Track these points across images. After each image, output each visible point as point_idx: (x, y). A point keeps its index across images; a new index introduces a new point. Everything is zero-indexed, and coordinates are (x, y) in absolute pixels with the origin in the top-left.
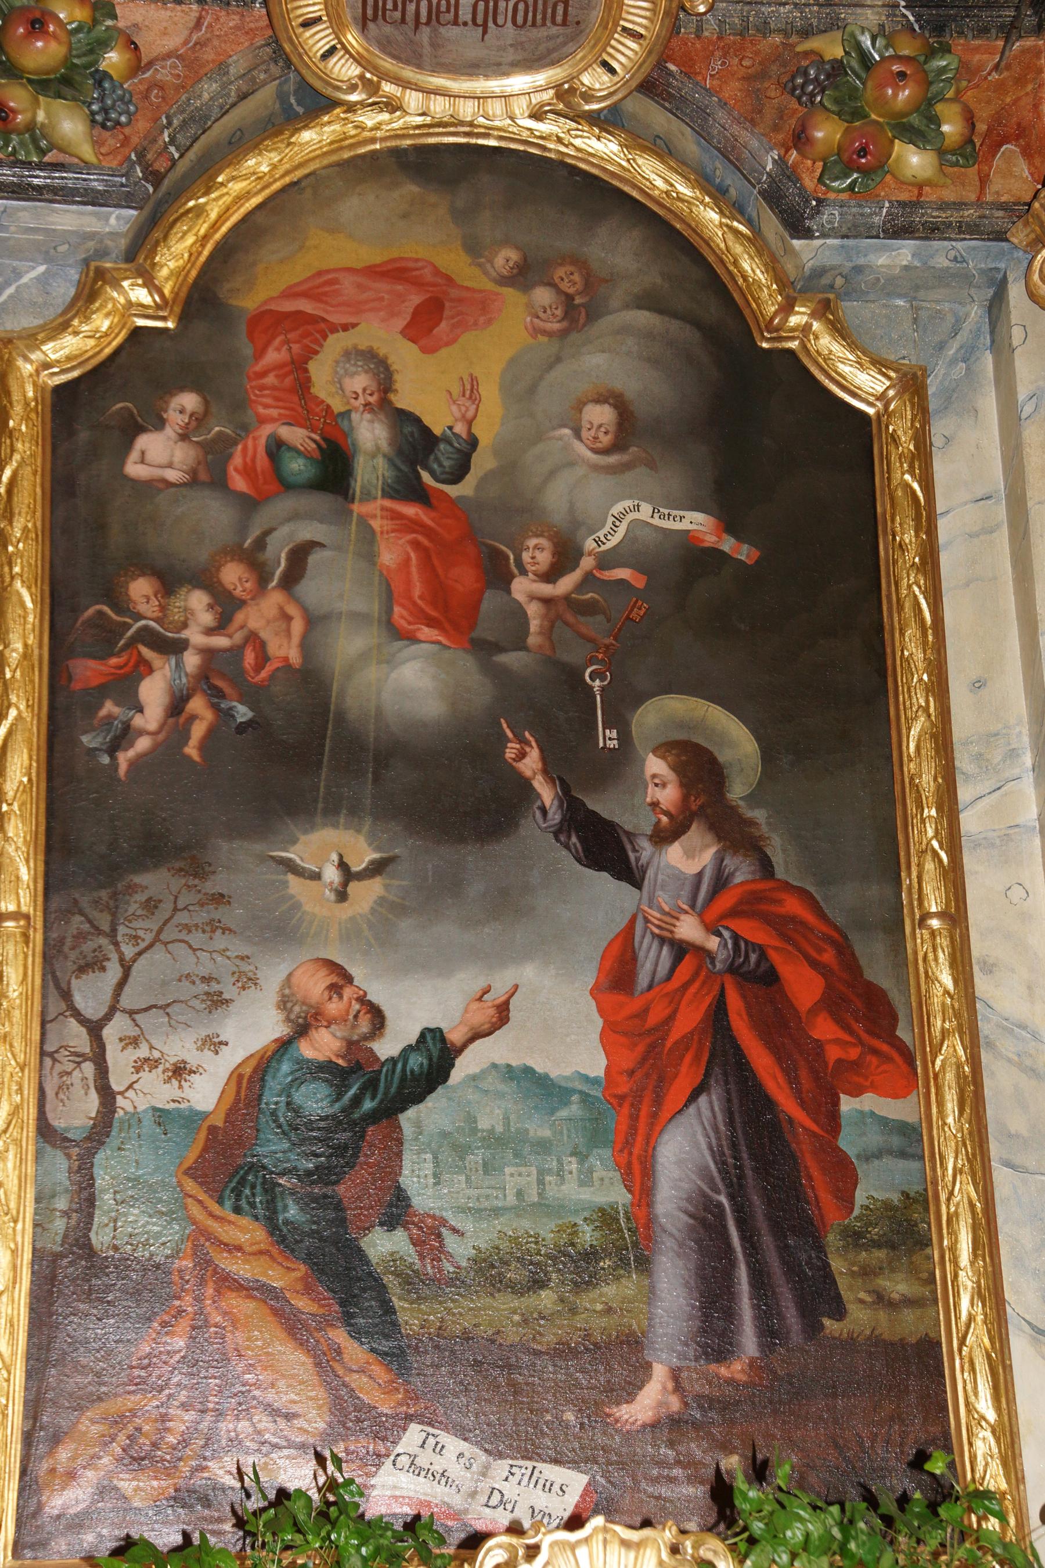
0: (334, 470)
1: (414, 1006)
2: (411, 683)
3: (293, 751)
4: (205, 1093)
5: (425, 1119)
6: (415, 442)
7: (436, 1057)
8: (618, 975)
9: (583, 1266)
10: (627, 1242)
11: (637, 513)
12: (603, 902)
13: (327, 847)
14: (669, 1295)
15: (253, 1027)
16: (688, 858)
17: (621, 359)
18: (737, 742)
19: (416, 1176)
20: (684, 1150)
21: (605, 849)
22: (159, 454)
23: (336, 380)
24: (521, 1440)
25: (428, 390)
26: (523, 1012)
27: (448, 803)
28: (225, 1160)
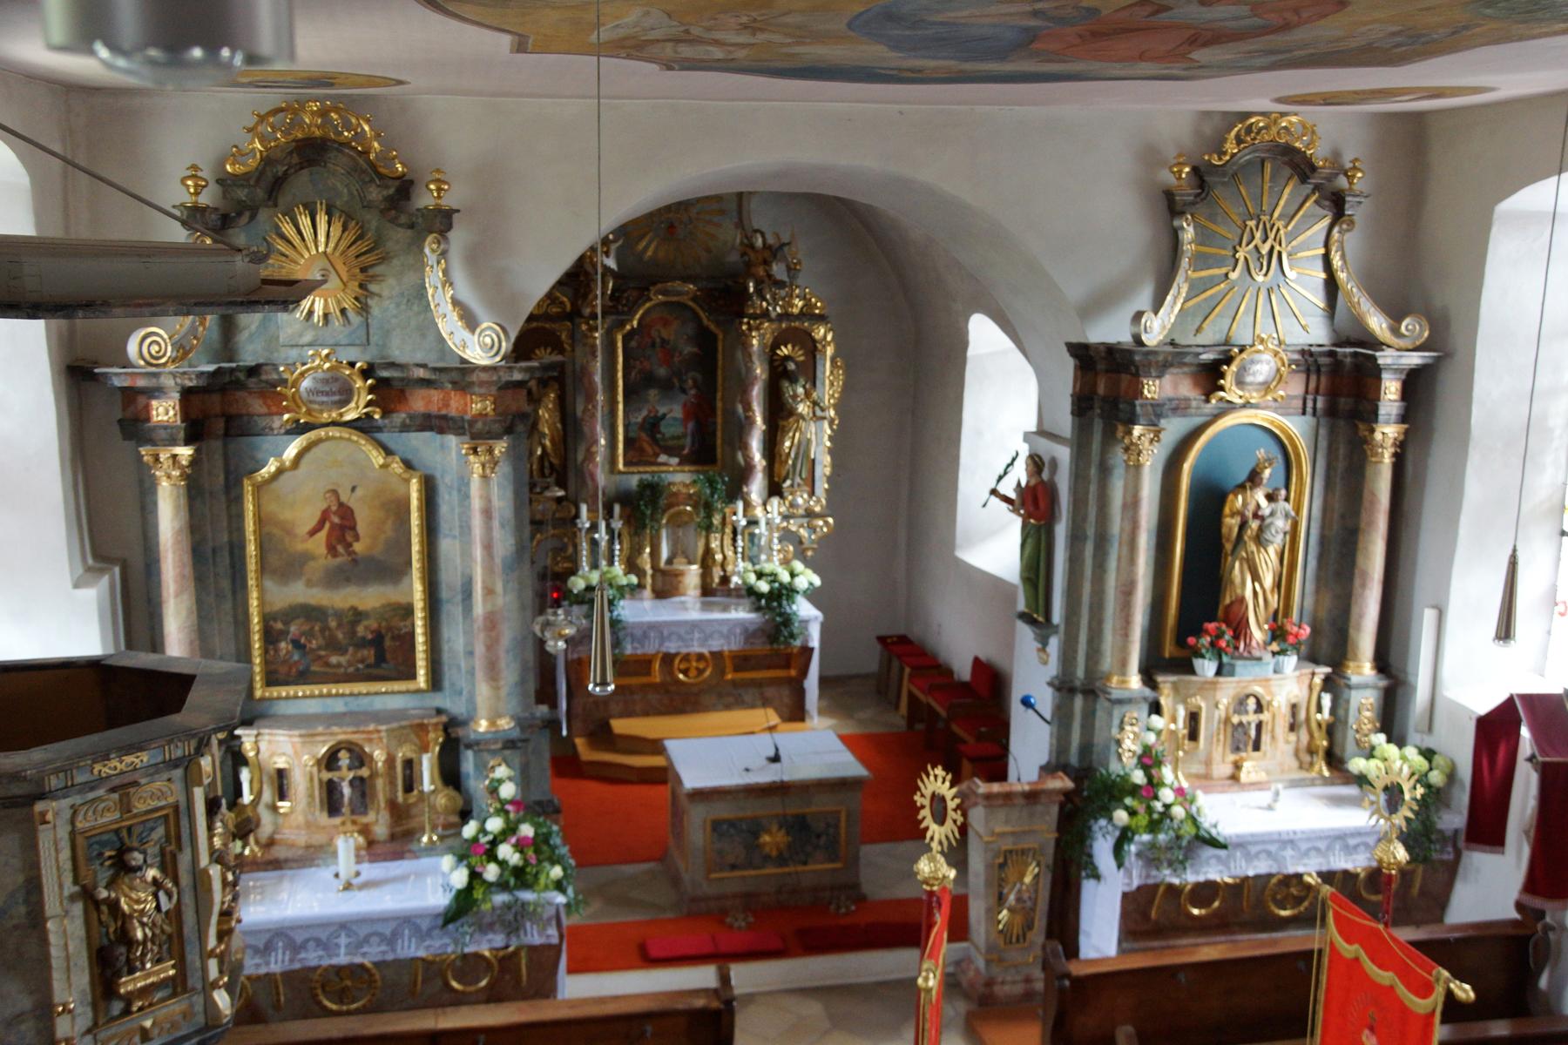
0: (653, 345)
1: (662, 410)
2: (662, 372)
3: (649, 380)
4: (640, 420)
5: (663, 423)
6: (663, 341)
7: (664, 415)
8: (685, 405)
9: (678, 438)
10: (684, 436)
11: (688, 349)
12: (683, 398)
13: (653, 393)
14: (688, 441)
15: (644, 413)
16: (693, 392)
17: (690, 329)
18: (699, 377)
19: (663, 429)
20: (691, 425)
21: (684, 391)
22: (633, 344)
23: (654, 333)
24: (671, 455)
25: (665, 334)
26: (673, 412)
27: (666, 387)
28: (642, 426)
